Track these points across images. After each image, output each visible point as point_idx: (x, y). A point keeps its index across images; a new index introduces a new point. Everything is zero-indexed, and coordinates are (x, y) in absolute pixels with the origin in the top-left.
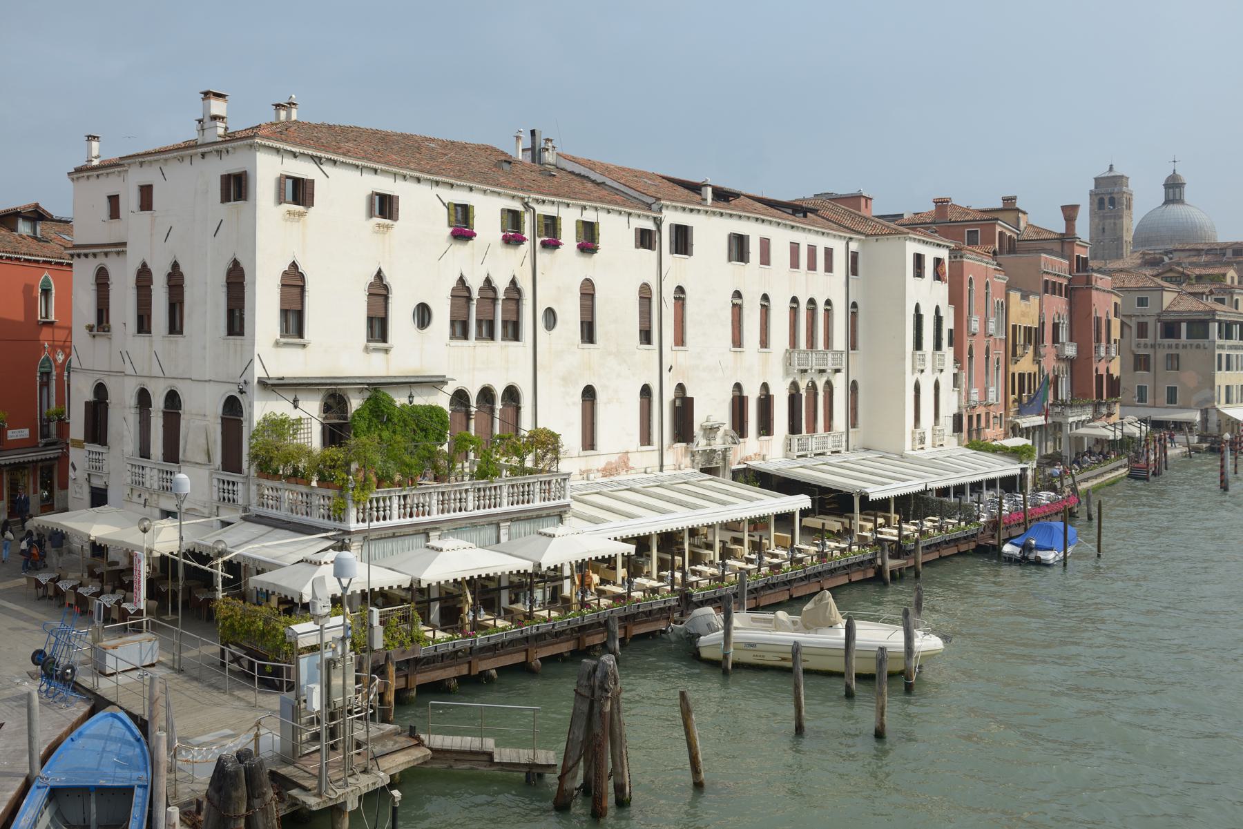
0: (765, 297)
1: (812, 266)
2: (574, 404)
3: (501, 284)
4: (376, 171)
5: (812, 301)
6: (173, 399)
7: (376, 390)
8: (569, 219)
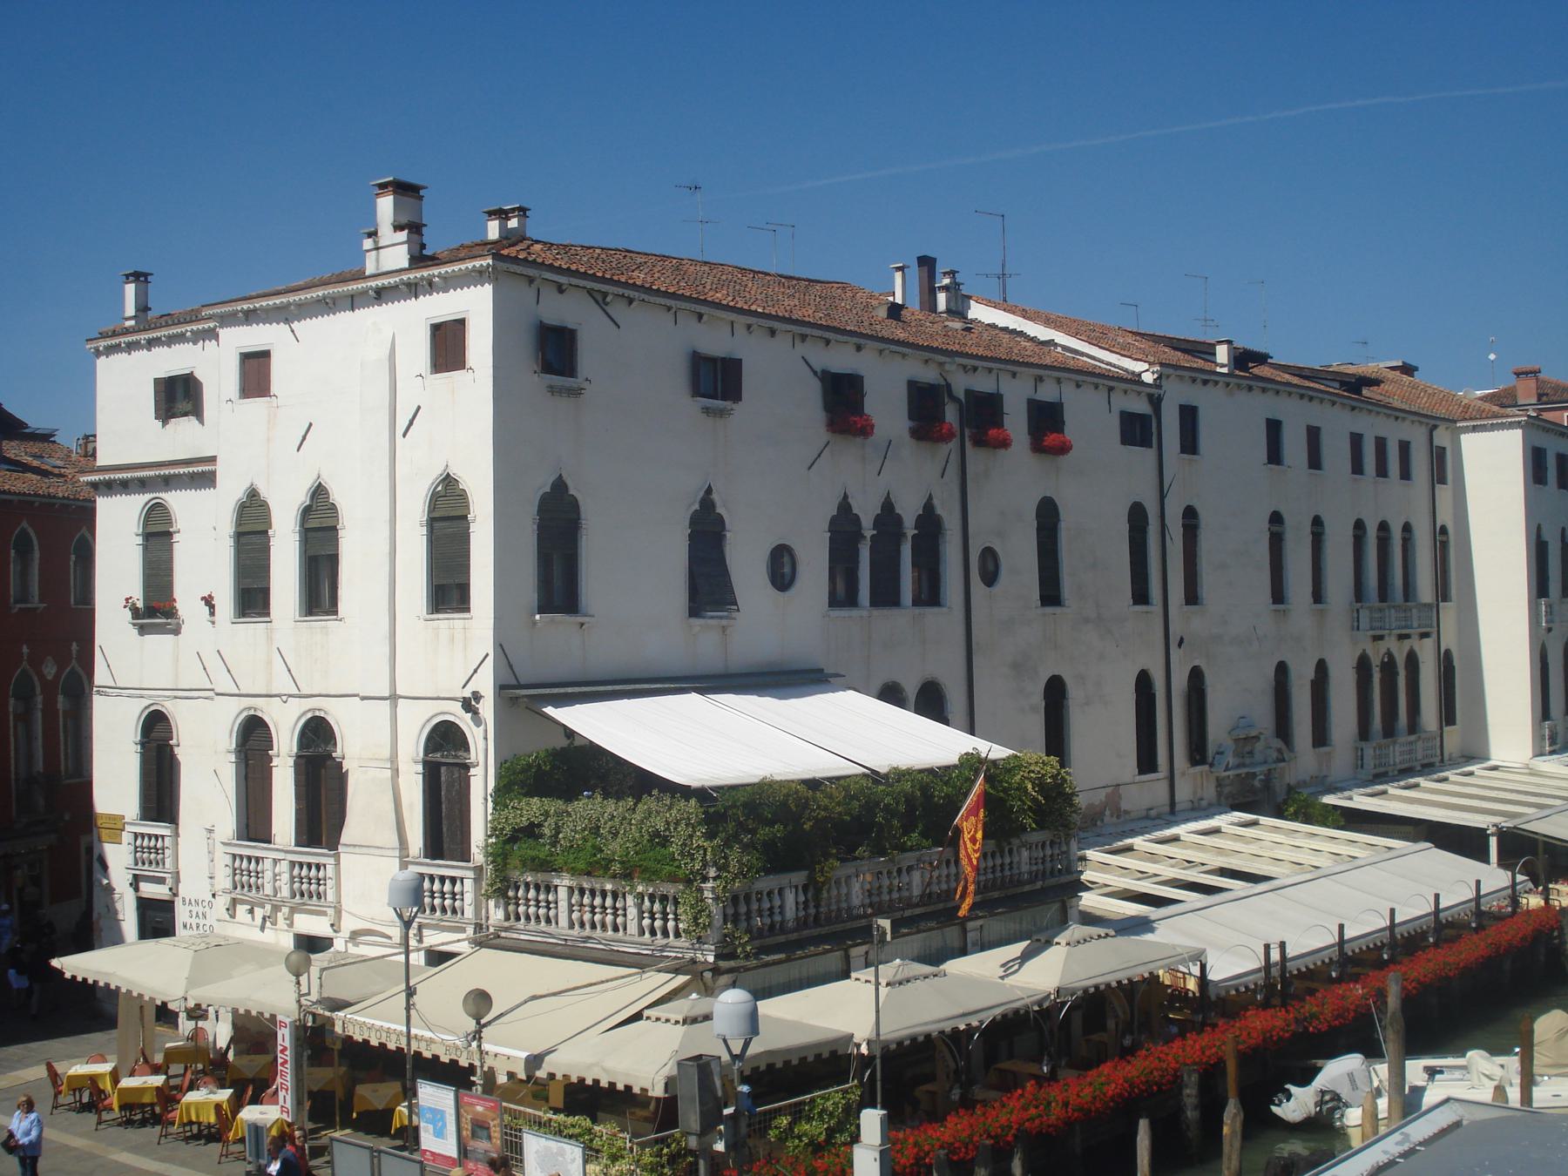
0: (1317, 522)
1: (1382, 471)
3: (909, 511)
5: (1383, 527)
6: (317, 733)
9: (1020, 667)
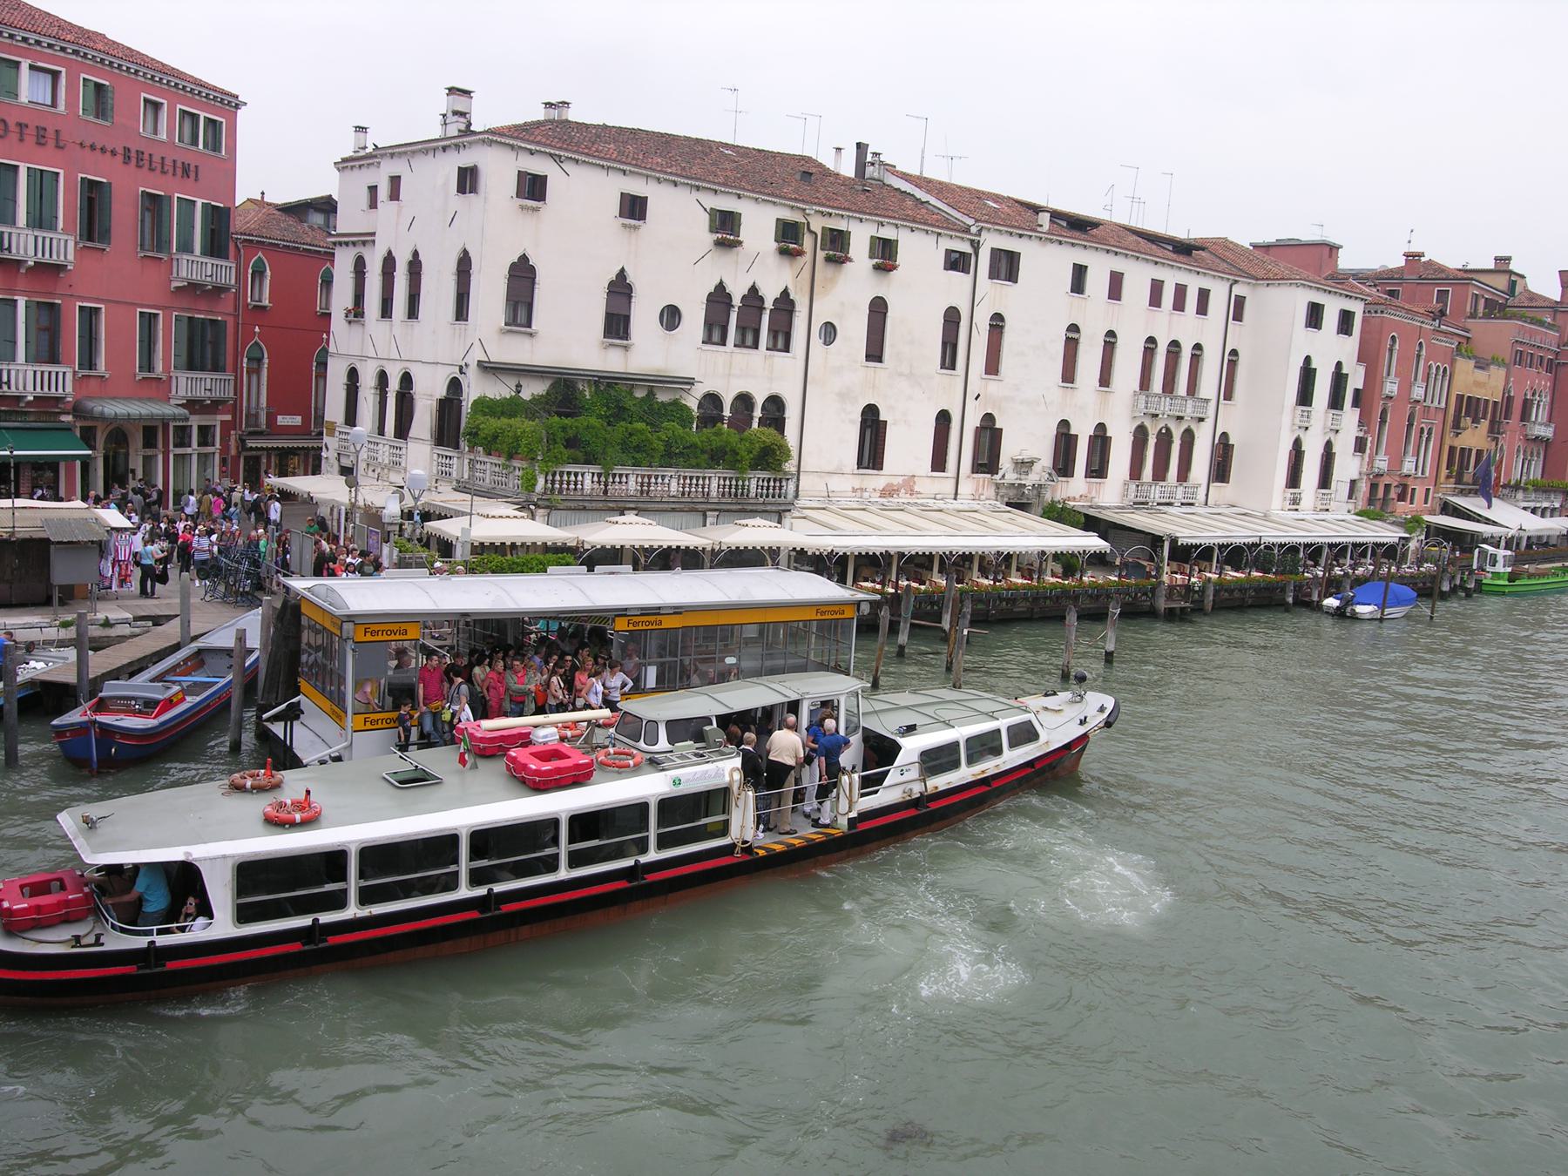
1: (1179, 305)
2: (852, 421)
3: (770, 295)
4: (624, 172)
5: (1175, 344)
7: (607, 383)
8: (861, 235)
9: (844, 396)
